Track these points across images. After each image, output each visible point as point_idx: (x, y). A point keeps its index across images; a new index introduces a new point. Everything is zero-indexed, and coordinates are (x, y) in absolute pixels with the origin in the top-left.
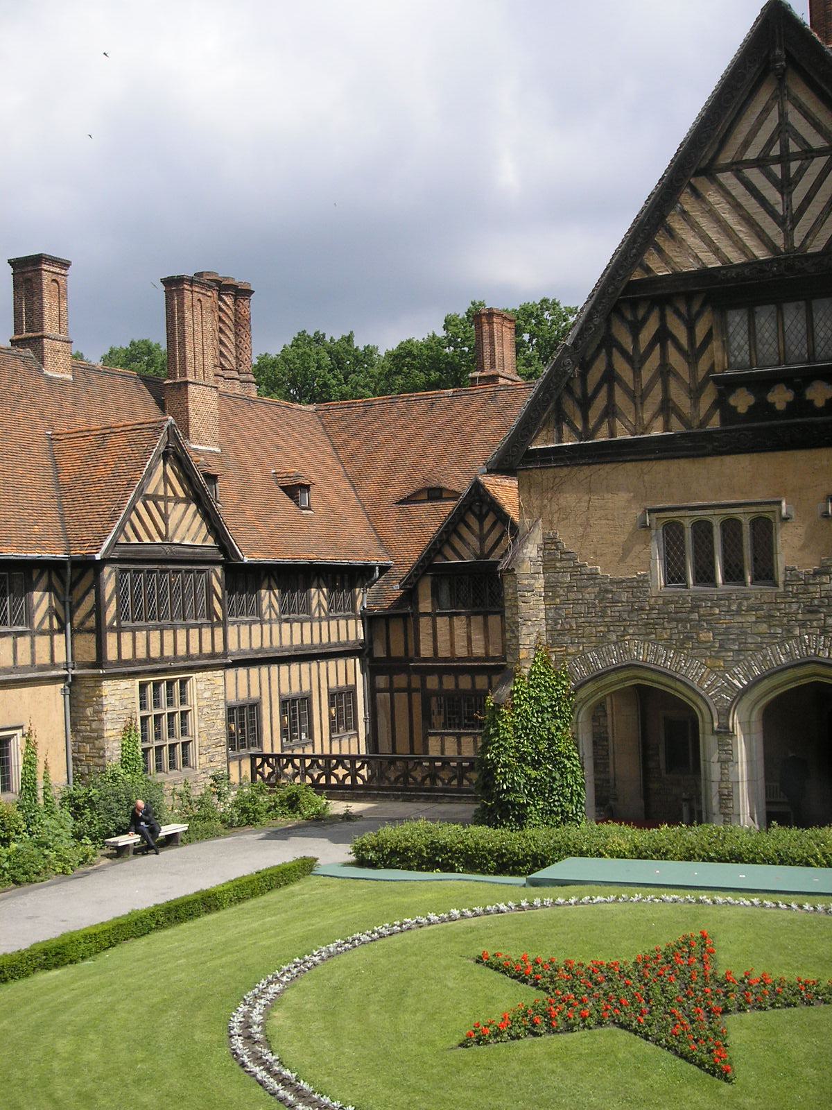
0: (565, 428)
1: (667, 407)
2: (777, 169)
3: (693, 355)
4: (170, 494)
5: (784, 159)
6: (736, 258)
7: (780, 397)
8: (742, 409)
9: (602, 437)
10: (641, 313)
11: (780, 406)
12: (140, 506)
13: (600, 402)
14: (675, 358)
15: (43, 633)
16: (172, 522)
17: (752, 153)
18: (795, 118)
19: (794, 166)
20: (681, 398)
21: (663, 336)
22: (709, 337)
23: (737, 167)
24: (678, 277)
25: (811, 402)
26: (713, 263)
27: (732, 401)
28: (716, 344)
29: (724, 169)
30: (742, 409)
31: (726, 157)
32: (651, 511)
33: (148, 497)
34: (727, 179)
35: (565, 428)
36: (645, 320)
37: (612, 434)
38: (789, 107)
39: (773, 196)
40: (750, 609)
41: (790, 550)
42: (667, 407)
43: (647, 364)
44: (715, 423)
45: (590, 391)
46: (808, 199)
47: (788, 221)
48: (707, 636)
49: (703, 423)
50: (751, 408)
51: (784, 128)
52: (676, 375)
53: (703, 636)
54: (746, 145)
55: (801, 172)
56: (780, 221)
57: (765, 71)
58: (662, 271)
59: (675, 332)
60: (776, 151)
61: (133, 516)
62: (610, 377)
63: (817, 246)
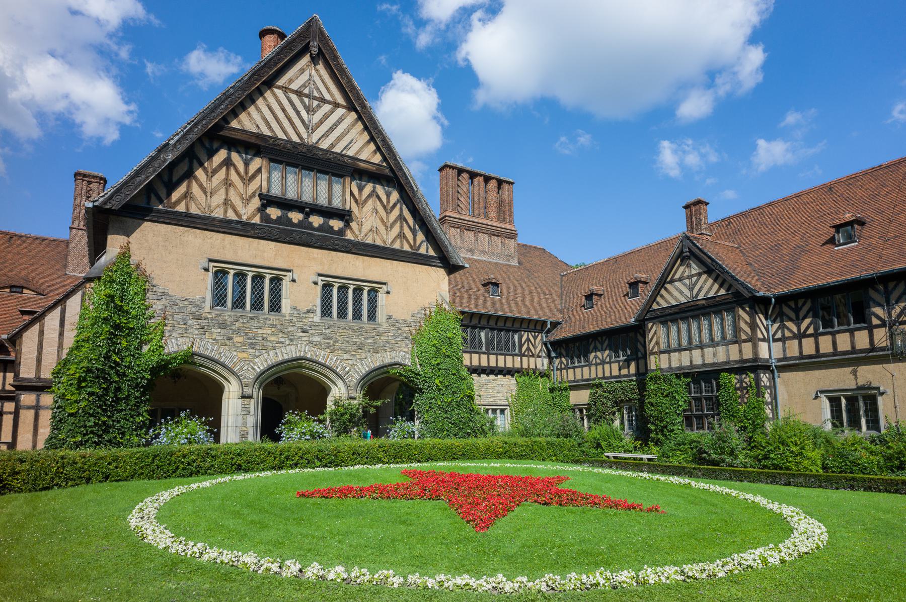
0: (153, 196)
1: (227, 202)
2: (306, 100)
3: (248, 179)
7: (296, 217)
8: (274, 217)
9: (181, 208)
10: (215, 145)
11: (295, 221)
14: (234, 177)
17: (294, 86)
21: (228, 163)
22: (259, 170)
23: (285, 89)
25: (311, 223)
26: (267, 133)
28: (265, 175)
29: (279, 87)
30: (274, 217)
31: (280, 82)
32: (211, 260)
34: (279, 92)
35: (153, 196)
36: (217, 151)
39: (304, 113)
40: (272, 326)
41: (290, 297)
42: (227, 202)
43: (216, 176)
44: (257, 220)
46: (321, 122)
48: (238, 339)
49: (249, 218)
50: (278, 217)
52: (235, 187)
53: (240, 339)
54: (291, 81)
55: (319, 107)
56: (307, 128)
57: (305, 50)
58: (234, 124)
59: (236, 163)
63: (324, 145)
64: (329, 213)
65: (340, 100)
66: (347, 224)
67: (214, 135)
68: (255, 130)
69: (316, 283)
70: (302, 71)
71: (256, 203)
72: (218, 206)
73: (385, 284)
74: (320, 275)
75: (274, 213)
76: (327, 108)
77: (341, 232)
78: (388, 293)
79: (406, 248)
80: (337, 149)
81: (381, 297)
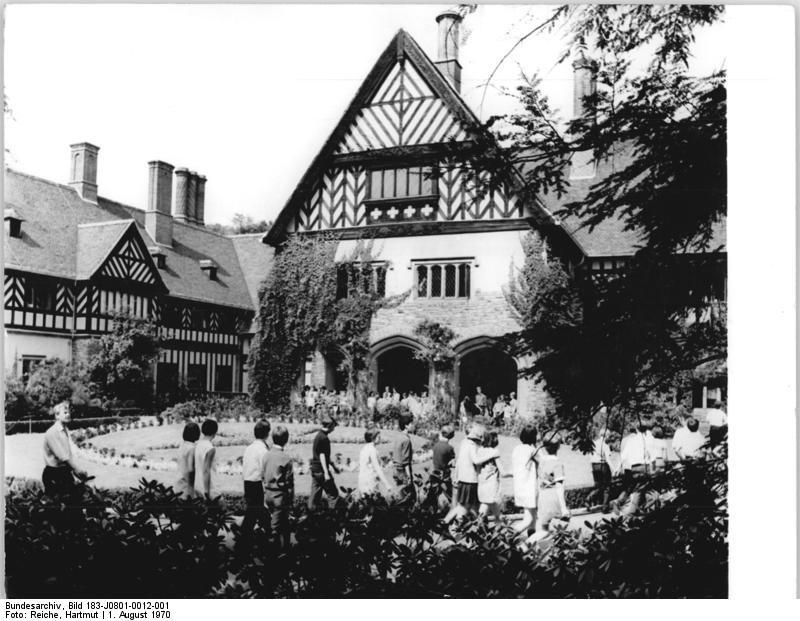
3: (357, 192)
4: (131, 256)
5: (401, 102)
6: (377, 146)
7: (393, 213)
10: (336, 171)
11: (393, 217)
12: (114, 259)
13: (315, 213)
15: (60, 314)
16: (132, 271)
17: (388, 98)
18: (407, 83)
19: (405, 105)
20: (350, 211)
21: (344, 182)
23: (380, 104)
24: (353, 154)
27: (372, 214)
31: (376, 100)
33: (120, 256)
34: (376, 109)
37: (320, 227)
38: (405, 77)
42: (343, 215)
44: (364, 224)
45: (312, 205)
47: (401, 131)
51: (402, 88)
56: (398, 131)
58: (345, 150)
60: (398, 98)
61: (110, 263)
62: (320, 201)
63: (412, 142)
64: (418, 203)
65: (427, 92)
66: (436, 208)
67: (329, 162)
68: (356, 149)
69: (410, 268)
70: (395, 79)
71: (362, 210)
72: (337, 221)
73: (473, 258)
74: (413, 260)
75: (376, 214)
76: (416, 104)
77: (433, 216)
78: (477, 266)
79: (497, 216)
80: (424, 140)
81: (473, 270)
